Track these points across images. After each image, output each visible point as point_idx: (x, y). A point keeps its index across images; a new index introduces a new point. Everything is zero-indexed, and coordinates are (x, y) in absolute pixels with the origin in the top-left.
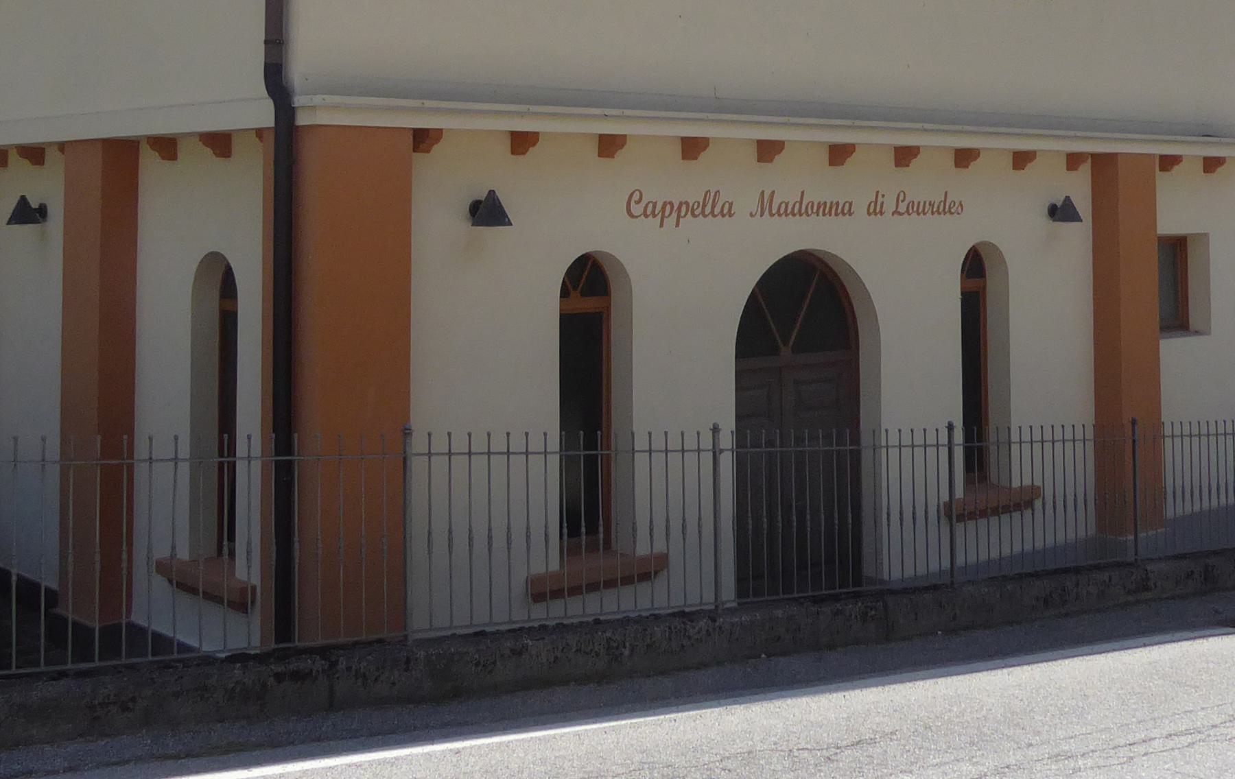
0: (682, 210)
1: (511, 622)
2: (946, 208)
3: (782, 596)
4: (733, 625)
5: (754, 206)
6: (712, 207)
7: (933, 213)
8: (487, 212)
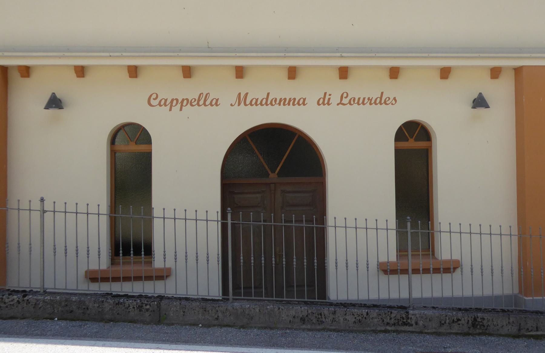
0: (183, 103)
1: (66, 289)
2: (381, 101)
3: (274, 299)
4: (38, 300)
5: (234, 99)
6: (203, 100)
7: (371, 104)
8: (55, 103)
